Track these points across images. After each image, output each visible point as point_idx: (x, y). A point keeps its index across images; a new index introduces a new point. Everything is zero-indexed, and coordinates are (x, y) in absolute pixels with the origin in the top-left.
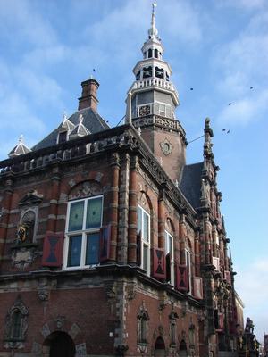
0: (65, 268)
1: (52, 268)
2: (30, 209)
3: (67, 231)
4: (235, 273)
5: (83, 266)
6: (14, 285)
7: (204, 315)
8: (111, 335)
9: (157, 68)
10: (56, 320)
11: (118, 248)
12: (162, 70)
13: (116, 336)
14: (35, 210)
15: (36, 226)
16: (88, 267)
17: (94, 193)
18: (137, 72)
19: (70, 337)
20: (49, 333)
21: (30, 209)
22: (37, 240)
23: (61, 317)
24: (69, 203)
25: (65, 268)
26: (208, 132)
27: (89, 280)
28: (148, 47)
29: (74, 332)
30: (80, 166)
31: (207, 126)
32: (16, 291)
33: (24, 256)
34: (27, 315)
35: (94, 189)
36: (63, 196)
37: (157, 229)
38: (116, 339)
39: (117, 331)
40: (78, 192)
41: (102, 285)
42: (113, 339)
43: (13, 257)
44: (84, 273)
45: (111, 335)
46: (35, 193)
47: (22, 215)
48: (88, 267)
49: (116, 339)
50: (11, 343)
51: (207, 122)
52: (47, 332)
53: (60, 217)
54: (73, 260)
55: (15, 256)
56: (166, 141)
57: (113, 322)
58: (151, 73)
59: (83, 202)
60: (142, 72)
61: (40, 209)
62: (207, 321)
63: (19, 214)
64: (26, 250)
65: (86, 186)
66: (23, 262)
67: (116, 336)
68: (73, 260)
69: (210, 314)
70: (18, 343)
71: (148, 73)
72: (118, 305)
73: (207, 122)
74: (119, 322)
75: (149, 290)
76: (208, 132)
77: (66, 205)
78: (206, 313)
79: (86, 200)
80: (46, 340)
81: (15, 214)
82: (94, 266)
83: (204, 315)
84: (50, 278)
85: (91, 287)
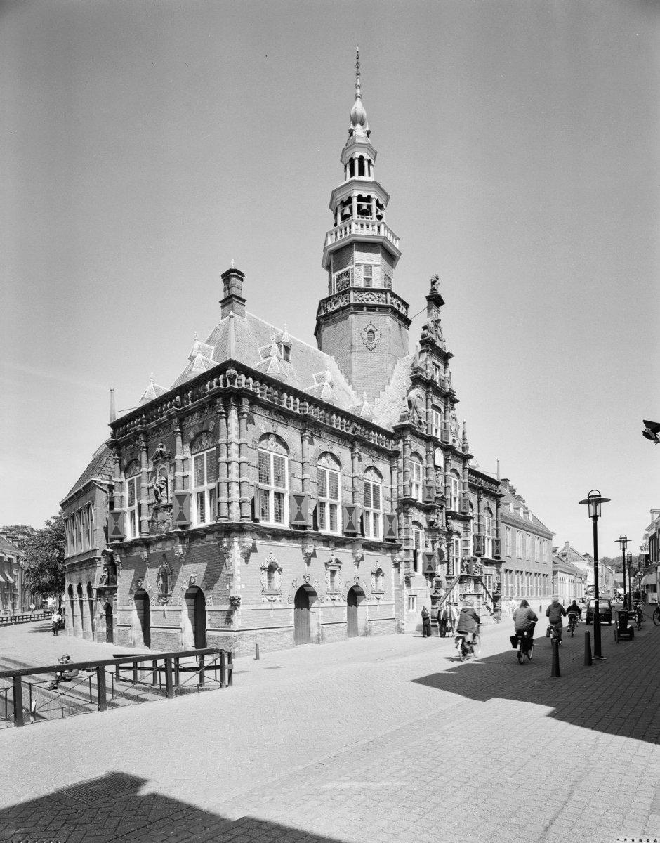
1: (183, 527)
6: (160, 545)
9: (360, 198)
12: (368, 199)
18: (333, 207)
26: (435, 300)
28: (348, 155)
32: (161, 550)
54: (203, 519)
56: (371, 328)
57: (229, 575)
67: (231, 588)
68: (203, 519)
69: (407, 556)
71: (347, 212)
72: (231, 560)
76: (435, 300)
84: (181, 537)
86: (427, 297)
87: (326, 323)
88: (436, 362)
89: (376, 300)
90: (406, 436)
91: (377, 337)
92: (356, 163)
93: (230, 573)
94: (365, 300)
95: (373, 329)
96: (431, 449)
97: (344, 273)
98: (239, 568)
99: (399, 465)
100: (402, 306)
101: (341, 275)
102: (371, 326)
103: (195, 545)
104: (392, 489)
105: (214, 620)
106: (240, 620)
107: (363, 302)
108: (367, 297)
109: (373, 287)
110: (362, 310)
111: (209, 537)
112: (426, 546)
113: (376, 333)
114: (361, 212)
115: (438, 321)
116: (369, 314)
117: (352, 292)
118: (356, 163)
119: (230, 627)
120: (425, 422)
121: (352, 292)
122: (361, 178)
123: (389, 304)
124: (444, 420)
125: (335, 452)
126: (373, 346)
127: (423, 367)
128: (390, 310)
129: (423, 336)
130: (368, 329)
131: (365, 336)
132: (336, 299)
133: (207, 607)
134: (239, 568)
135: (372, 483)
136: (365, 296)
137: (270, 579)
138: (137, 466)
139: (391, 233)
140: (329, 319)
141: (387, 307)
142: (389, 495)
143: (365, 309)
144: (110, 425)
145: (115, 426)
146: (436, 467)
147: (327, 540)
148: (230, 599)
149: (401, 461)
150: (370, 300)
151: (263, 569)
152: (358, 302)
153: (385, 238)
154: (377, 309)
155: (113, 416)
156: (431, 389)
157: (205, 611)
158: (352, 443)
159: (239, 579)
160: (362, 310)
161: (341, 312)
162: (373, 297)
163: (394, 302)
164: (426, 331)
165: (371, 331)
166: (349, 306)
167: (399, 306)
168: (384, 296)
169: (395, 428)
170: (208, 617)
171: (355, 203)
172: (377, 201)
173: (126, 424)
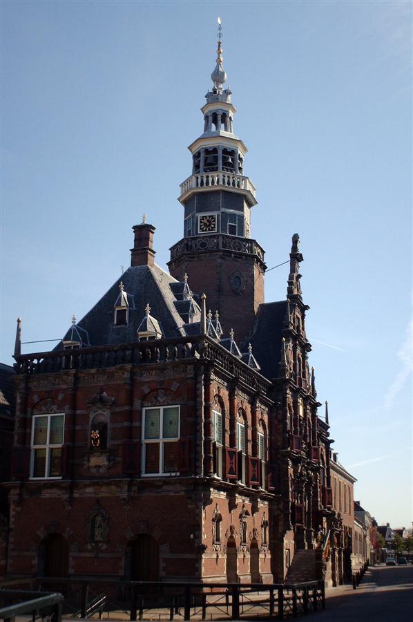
4: (332, 441)
7: (278, 509)
8: (192, 536)
15: (109, 432)
17: (170, 402)
26: (296, 257)
27: (170, 488)
31: (295, 248)
32: (93, 495)
35: (170, 398)
36: (137, 402)
37: (227, 427)
38: (196, 540)
40: (153, 399)
41: (183, 493)
44: (166, 481)
45: (192, 536)
48: (168, 474)
50: (93, 544)
51: (296, 239)
53: (136, 424)
54: (153, 467)
55: (89, 461)
58: (216, 159)
61: (112, 413)
63: (86, 417)
64: (101, 456)
70: (100, 544)
73: (296, 239)
82: (173, 474)
83: (278, 509)
87: (190, 261)
97: (210, 216)
99: (279, 416)
101: (206, 217)
109: (237, 236)
113: (242, 279)
115: (299, 276)
117: (221, 238)
132: (203, 241)
160: (230, 256)
170: (162, 564)
171: (220, 154)
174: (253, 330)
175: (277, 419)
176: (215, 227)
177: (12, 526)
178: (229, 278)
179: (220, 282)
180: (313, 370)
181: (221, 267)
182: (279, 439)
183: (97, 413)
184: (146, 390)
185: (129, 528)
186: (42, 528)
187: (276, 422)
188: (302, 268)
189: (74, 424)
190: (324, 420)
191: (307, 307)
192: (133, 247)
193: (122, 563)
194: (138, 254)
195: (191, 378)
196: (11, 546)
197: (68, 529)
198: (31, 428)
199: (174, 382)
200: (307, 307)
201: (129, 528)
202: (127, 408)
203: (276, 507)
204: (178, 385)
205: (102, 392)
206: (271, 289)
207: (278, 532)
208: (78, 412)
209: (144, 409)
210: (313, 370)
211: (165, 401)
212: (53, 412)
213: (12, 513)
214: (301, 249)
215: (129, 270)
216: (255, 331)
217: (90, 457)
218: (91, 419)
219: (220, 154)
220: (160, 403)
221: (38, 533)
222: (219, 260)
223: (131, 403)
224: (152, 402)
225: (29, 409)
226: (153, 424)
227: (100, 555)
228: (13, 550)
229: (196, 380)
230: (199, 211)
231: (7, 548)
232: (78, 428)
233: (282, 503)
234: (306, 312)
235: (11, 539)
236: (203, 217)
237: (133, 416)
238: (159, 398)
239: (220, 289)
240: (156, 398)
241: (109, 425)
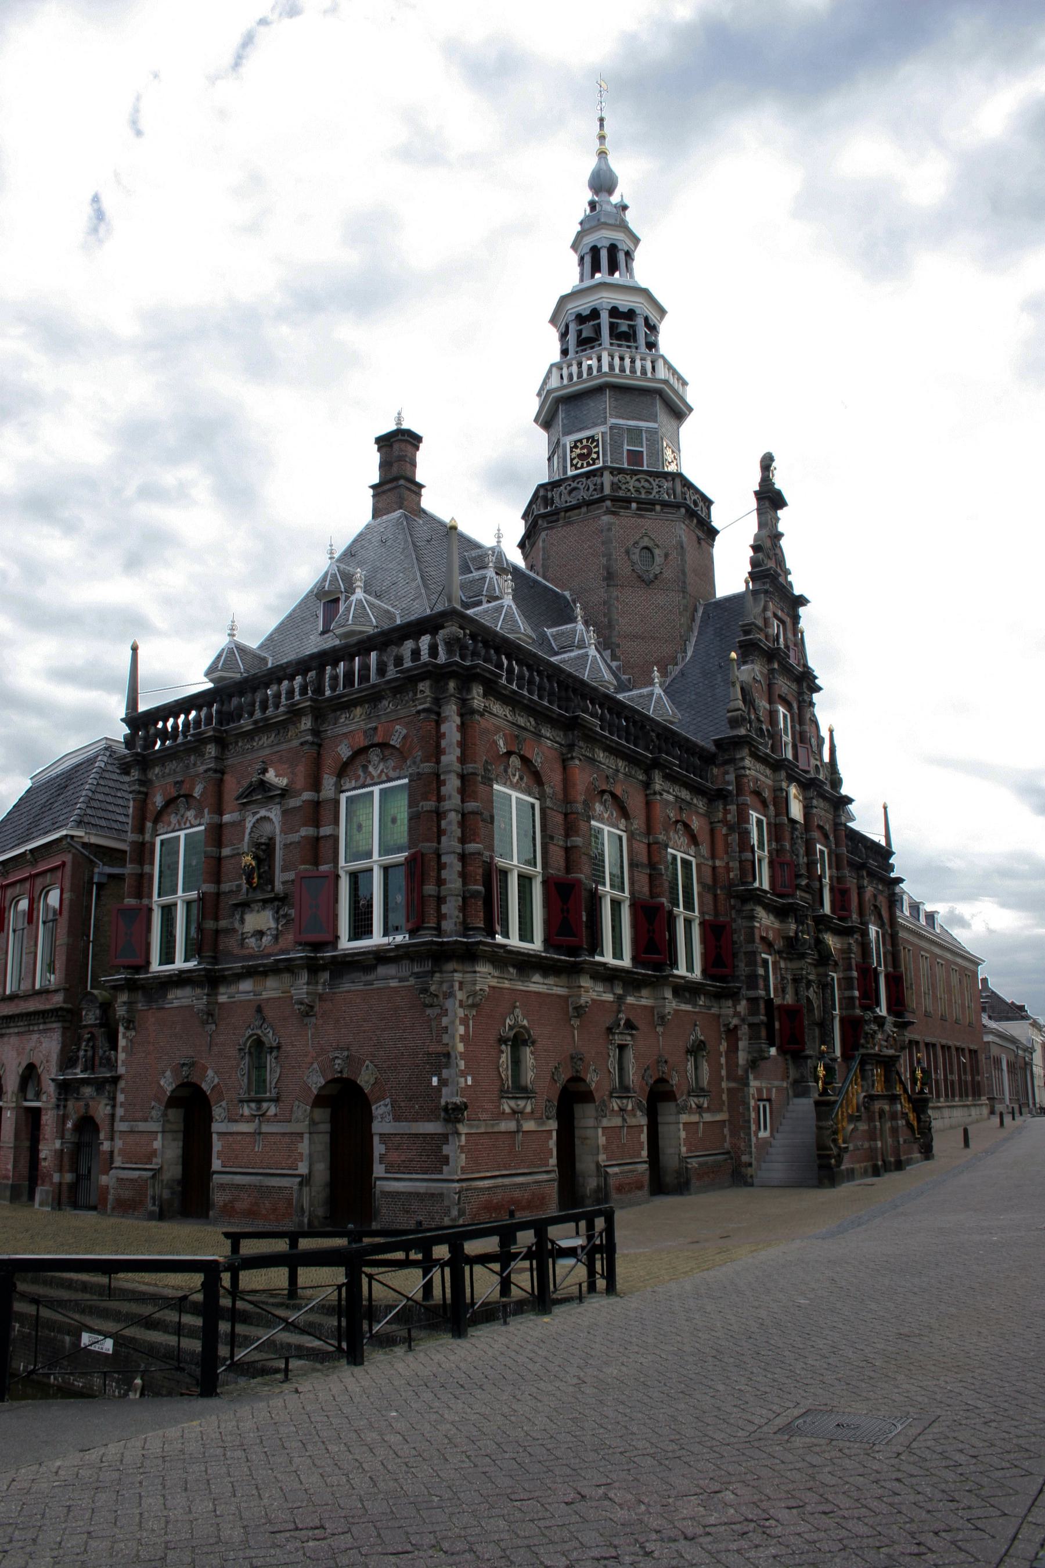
0: (346, 944)
1: (317, 946)
2: (263, 813)
3: (342, 862)
5: (377, 939)
6: (246, 986)
7: (736, 1014)
8: (435, 1081)
10: (331, 1055)
11: (440, 900)
13: (443, 1082)
14: (274, 813)
15: (279, 854)
16: (385, 940)
17: (392, 774)
19: (360, 1089)
20: (322, 1081)
21: (263, 813)
22: (284, 883)
23: (342, 1049)
24: (343, 797)
25: (346, 944)
26: (770, 499)
27: (390, 970)
29: (365, 1079)
30: (358, 711)
32: (251, 997)
33: (259, 920)
34: (278, 1048)
35: (391, 763)
36: (328, 782)
38: (444, 1090)
39: (445, 1073)
42: (438, 1089)
43: (237, 925)
44: (380, 957)
45: (435, 1081)
46: (271, 776)
47: (249, 825)
48: (385, 940)
49: (444, 1090)
50: (253, 1105)
51: (767, 463)
52: (316, 1081)
53: (325, 831)
55: (242, 921)
56: (646, 542)
57: (438, 1055)
58: (598, 329)
59: (372, 793)
60: (573, 327)
61: (285, 813)
62: (745, 1028)
63: (240, 824)
64: (264, 909)
65: (374, 756)
66: (260, 934)
69: (753, 1011)
70: (265, 1105)
72: (445, 1021)
73: (767, 463)
74: (448, 1055)
75: (537, 978)
76: (770, 499)
77: (337, 802)
78: (742, 1007)
79: (376, 789)
80: (317, 1096)
81: (233, 824)
84: (313, 968)
85: (394, 983)
86: (756, 493)
87: (551, 528)
88: (779, 613)
89: (654, 493)
90: (743, 759)
91: (659, 560)
92: (604, 255)
93: (444, 1050)
94: (632, 490)
95: (650, 545)
96: (784, 785)
97: (588, 439)
98: (463, 1039)
99: (729, 817)
100: (701, 504)
101: (581, 441)
102: (646, 539)
103: (346, 986)
104: (714, 868)
105: (394, 1156)
106: (463, 1156)
107: (629, 494)
108: (637, 484)
109: (645, 468)
110: (629, 508)
111: (382, 970)
112: (784, 990)
113: (657, 551)
114: (617, 335)
116: (641, 516)
117: (606, 474)
118: (604, 255)
119: (441, 1172)
120: (768, 730)
121: (606, 474)
122: (609, 279)
123: (680, 500)
124: (797, 727)
125: (618, 791)
126: (651, 576)
127: (760, 623)
128: (683, 510)
129: (754, 563)
130: (642, 545)
131: (635, 557)
132: (574, 485)
133: (377, 1127)
134: (463, 1039)
135: (679, 855)
136: (632, 483)
137: (516, 1062)
138: (188, 809)
139: (675, 372)
140: (557, 520)
141: (677, 506)
142: (709, 881)
143: (634, 505)
144: (122, 720)
145: (136, 721)
146: (793, 822)
147: (609, 976)
148: (446, 1109)
149: (733, 808)
150: (643, 491)
151: (502, 1041)
152: (621, 494)
153: (666, 382)
154: (658, 508)
155: (133, 701)
156: (776, 666)
157: (371, 1136)
158: (647, 772)
159: (462, 1064)
160: (629, 508)
161: (584, 509)
162: (647, 485)
163: (687, 496)
164: (760, 555)
165: (646, 548)
166: (602, 500)
167: (695, 503)
168: (670, 484)
169: (718, 743)
170: (378, 1148)
171: (605, 319)
172: (646, 319)
173: (165, 721)
174: (685, 652)
175: (724, 822)
176: (598, 458)
177: (121, 1070)
178: (627, 552)
179: (609, 560)
180: (831, 732)
181: (610, 530)
182: (731, 864)
183: (258, 816)
184: (344, 752)
185: (315, 1065)
186: (168, 1073)
187: (724, 831)
188: (786, 520)
189: (219, 844)
190: (883, 843)
191: (802, 601)
192: (376, 480)
193: (304, 1147)
194: (384, 492)
195: (424, 710)
196: (120, 1112)
197: (210, 1073)
198: (152, 863)
199: (398, 727)
200: (802, 601)
201: (315, 1065)
202: (307, 796)
203: (731, 1011)
204: (405, 731)
205: (264, 771)
206: (731, 573)
207: (737, 1065)
208: (227, 818)
209: (343, 797)
210: (831, 732)
211: (382, 771)
212: (188, 825)
213: (122, 1042)
214: (780, 481)
215: (368, 527)
216: (689, 654)
217: (243, 913)
218: (248, 831)
219: (605, 319)
220: (372, 778)
221: (162, 1083)
222: (606, 518)
223: (316, 785)
224: (357, 778)
225: (149, 825)
226: (360, 827)
227: (265, 1129)
228: (122, 1119)
229: (438, 714)
230: (566, 433)
231: (113, 1116)
232: (226, 852)
233: (744, 1003)
234: (802, 611)
235: (121, 1098)
236: (576, 442)
237: (319, 812)
238: (371, 769)
239: (608, 573)
240: (365, 768)
241: (278, 839)
